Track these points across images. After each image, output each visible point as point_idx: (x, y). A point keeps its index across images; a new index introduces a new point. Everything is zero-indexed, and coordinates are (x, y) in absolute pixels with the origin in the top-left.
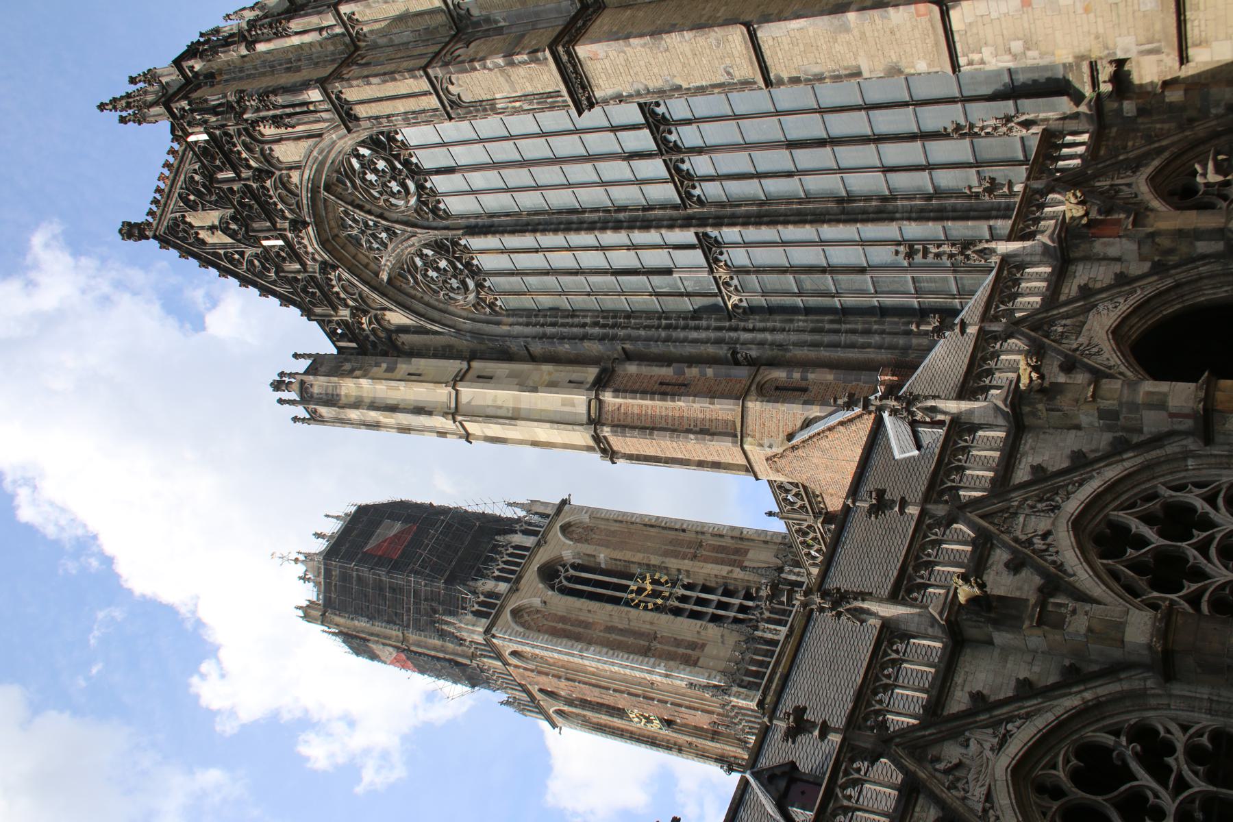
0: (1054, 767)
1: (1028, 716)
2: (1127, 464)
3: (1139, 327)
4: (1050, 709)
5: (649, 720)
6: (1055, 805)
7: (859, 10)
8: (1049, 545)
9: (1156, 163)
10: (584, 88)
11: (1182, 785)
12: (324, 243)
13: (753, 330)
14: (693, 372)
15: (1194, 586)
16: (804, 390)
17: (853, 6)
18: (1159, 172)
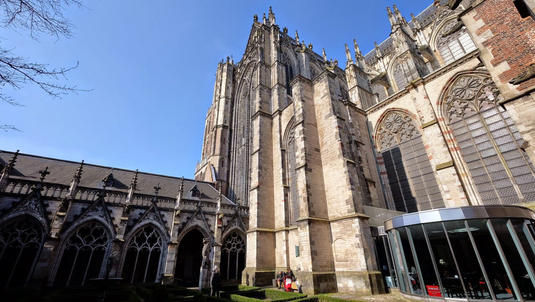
0: (98, 225)
1: (107, 220)
2: (164, 231)
3: (200, 230)
4: (108, 223)
5: (208, 138)
6: (90, 226)
7: (259, 172)
8: (146, 219)
9: (241, 229)
10: (254, 118)
11: (94, 247)
12: (248, 64)
13: (236, 155)
14: (227, 144)
15: (137, 245)
16: (222, 166)
17: (260, 171)
18: (239, 230)
